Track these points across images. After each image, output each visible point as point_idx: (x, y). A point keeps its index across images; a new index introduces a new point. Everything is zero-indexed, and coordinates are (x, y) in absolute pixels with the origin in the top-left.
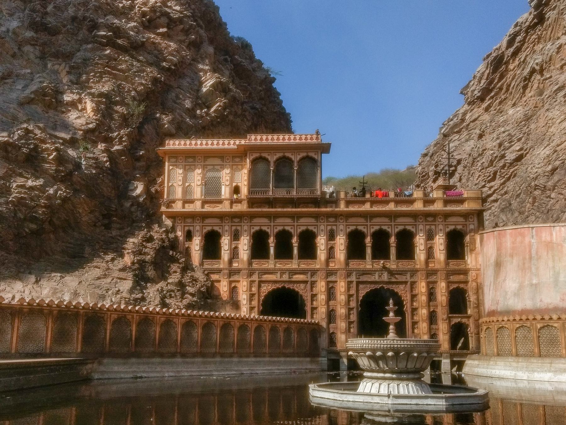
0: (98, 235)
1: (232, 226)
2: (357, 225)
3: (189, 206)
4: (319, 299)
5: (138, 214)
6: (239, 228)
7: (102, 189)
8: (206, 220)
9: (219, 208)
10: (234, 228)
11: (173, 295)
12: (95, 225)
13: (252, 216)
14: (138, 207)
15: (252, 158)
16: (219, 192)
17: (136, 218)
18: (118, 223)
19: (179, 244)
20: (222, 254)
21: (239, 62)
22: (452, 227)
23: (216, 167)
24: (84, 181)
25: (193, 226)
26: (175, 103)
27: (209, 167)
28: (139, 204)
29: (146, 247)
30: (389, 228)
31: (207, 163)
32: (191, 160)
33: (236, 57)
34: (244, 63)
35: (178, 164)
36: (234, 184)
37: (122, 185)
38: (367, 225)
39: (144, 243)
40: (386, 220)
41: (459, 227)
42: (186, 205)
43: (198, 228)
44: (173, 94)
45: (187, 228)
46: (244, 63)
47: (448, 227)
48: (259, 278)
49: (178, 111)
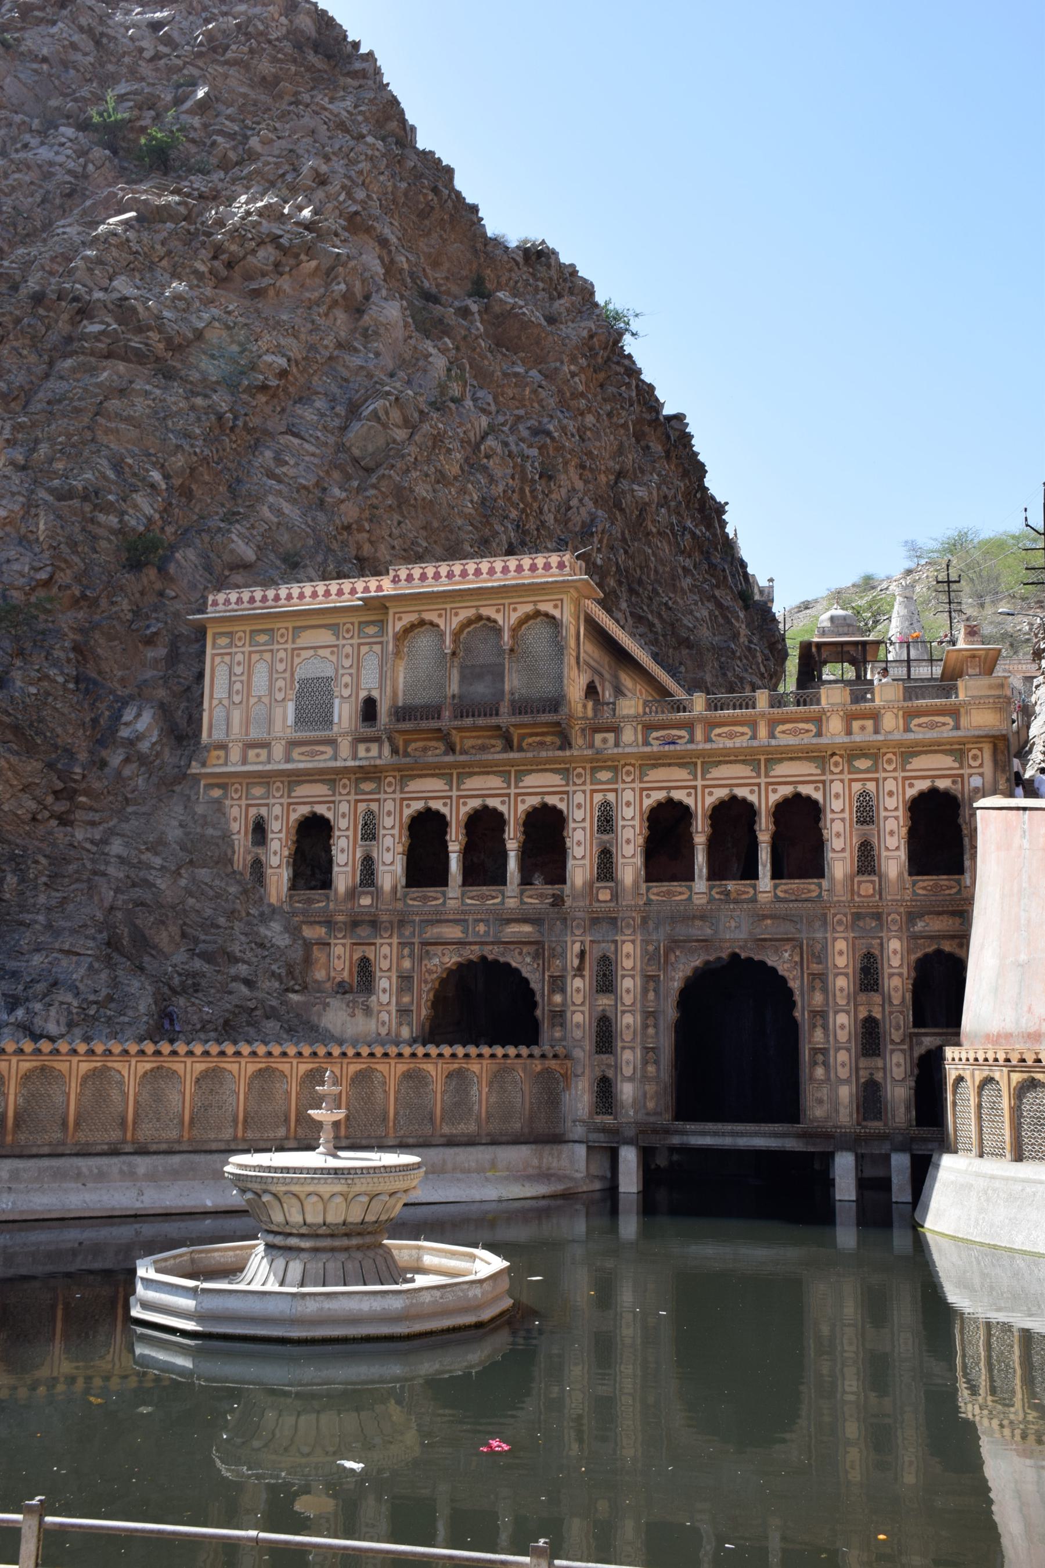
0: (42, 841)
1: (357, 801)
2: (669, 789)
3: (258, 755)
4: (569, 989)
5: (140, 782)
6: (374, 806)
7: (53, 731)
8: (297, 788)
9: (324, 759)
10: (362, 807)
11: (204, 983)
12: (34, 819)
13: (406, 774)
14: (141, 765)
15: (399, 625)
16: (327, 721)
17: (133, 792)
18: (91, 809)
19: (234, 852)
20: (334, 874)
21: (508, 307)
22: (924, 785)
23: (321, 652)
24: (9, 715)
25: (267, 805)
26: (271, 475)
27: (305, 654)
28: (143, 760)
29: (149, 867)
30: (752, 792)
31: (301, 642)
32: (263, 638)
33: (500, 294)
34: (521, 307)
35: (234, 650)
36: (363, 694)
37: (107, 713)
38: (695, 787)
39: (147, 857)
40: (742, 771)
41: (942, 784)
42: (252, 753)
43: (277, 810)
44: (269, 454)
45: (253, 811)
46: (521, 307)
47: (911, 785)
48: (420, 935)
49: (271, 499)
